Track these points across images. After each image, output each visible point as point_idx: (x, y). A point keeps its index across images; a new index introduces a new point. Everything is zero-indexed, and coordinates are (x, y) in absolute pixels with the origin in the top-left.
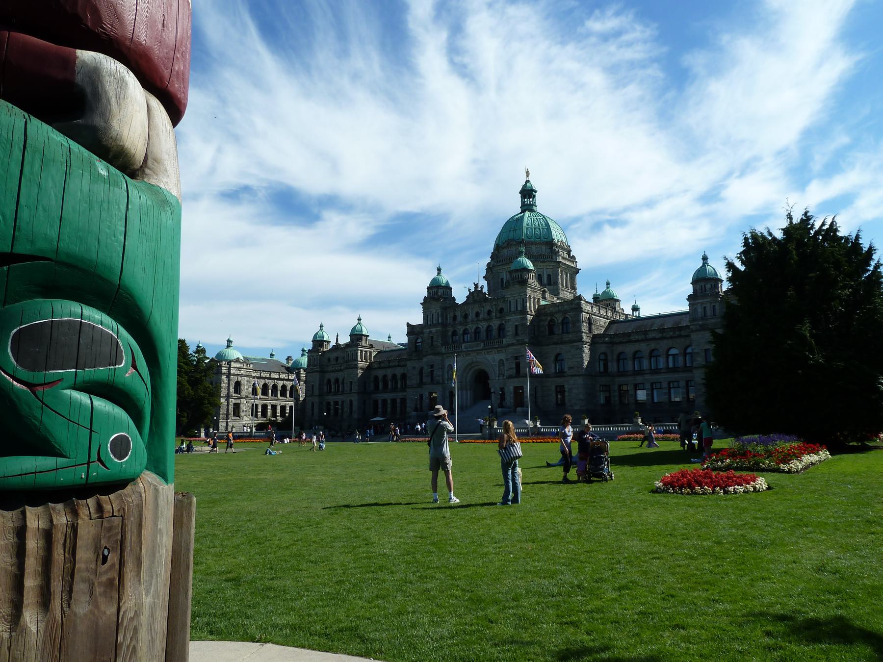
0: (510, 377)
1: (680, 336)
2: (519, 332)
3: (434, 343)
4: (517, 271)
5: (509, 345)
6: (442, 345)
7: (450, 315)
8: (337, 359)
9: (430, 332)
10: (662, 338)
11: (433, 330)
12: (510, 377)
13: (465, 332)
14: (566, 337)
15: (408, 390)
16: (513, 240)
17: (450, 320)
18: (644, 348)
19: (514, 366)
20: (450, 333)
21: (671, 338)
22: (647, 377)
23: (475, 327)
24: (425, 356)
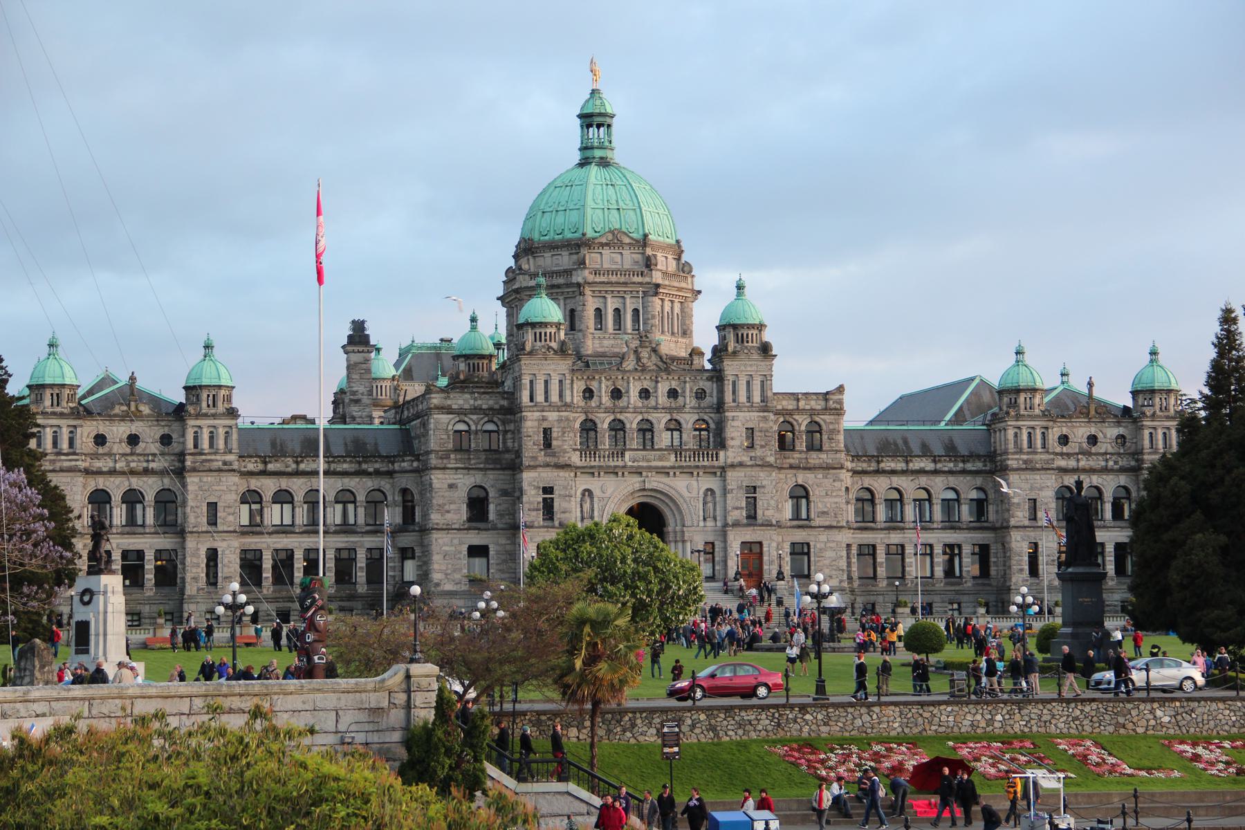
0: (736, 524)
1: (964, 472)
2: (758, 442)
3: (554, 443)
4: (752, 326)
5: (732, 466)
6: (575, 450)
7: (579, 386)
8: (133, 440)
9: (544, 419)
10: (936, 472)
11: (552, 416)
12: (736, 524)
13: (618, 427)
14: (815, 458)
15: (435, 535)
16: (620, 231)
17: (578, 399)
18: (909, 486)
19: (744, 504)
20: (577, 425)
21: (951, 472)
22: (910, 535)
23: (640, 417)
24: (535, 467)
